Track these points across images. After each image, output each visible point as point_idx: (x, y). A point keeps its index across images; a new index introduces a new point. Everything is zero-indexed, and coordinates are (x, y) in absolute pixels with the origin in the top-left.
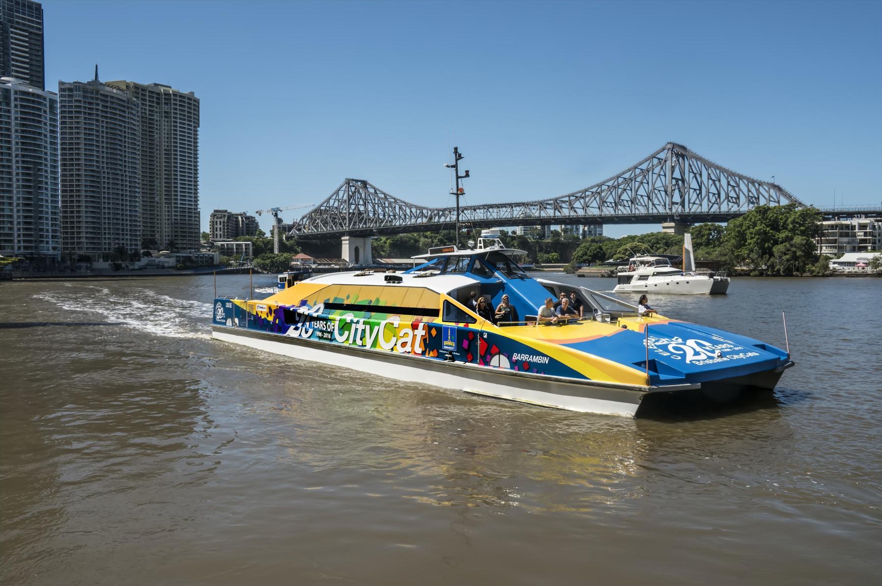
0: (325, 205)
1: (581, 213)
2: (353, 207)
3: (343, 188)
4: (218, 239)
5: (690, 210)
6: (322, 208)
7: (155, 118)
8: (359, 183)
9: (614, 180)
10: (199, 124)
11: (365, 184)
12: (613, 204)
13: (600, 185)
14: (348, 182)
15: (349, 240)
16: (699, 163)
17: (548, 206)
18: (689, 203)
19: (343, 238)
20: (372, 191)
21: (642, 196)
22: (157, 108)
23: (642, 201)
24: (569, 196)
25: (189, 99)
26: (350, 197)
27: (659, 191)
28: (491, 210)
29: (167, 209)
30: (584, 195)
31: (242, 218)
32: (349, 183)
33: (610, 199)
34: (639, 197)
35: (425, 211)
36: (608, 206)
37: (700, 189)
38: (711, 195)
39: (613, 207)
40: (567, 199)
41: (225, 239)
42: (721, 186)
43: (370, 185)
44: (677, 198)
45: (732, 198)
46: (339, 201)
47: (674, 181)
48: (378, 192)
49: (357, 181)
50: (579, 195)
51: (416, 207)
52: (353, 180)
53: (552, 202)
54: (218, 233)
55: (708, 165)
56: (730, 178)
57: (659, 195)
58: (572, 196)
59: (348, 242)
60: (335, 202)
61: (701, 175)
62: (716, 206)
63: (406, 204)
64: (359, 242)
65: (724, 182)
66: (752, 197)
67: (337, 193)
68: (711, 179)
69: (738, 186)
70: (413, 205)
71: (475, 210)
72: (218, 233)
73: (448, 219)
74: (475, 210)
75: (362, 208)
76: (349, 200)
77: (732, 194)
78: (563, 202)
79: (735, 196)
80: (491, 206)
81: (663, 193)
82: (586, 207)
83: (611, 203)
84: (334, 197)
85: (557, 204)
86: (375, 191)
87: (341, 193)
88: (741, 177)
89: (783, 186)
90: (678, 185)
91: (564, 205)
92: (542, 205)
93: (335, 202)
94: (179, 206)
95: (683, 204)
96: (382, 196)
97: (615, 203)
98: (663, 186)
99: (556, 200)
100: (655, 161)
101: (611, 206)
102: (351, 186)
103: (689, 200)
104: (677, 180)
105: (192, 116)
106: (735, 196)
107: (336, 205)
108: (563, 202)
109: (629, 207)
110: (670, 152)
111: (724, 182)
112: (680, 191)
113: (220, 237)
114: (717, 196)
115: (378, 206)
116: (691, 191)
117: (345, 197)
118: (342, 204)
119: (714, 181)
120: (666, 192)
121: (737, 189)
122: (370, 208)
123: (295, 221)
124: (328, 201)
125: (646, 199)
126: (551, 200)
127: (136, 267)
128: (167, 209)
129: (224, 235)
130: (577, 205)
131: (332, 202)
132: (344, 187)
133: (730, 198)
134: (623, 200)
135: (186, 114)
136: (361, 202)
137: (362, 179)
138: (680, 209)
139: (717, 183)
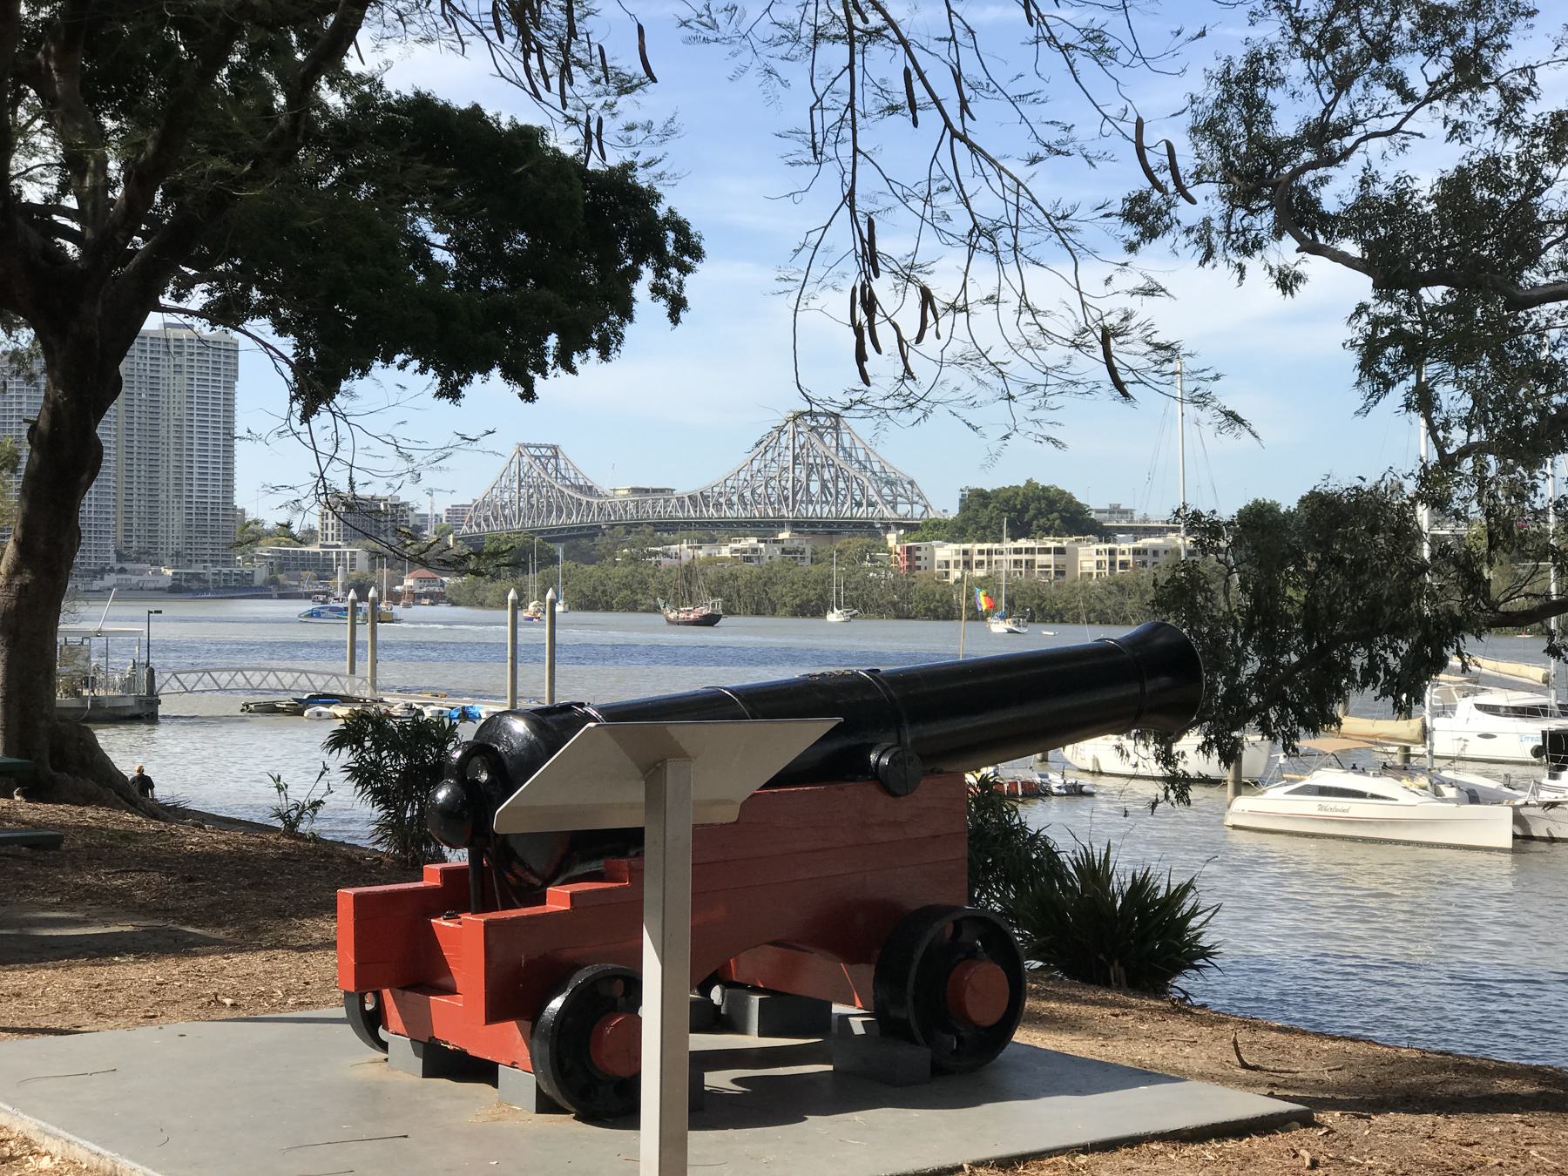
4: (330, 542)
7: (161, 375)
8: (543, 450)
10: (236, 377)
22: (164, 360)
25: (214, 342)
29: (176, 505)
31: (385, 505)
41: (340, 543)
49: (538, 447)
54: (330, 532)
72: (330, 532)
94: (194, 500)
105: (222, 366)
127: (95, 587)
128: (176, 505)
129: (339, 535)
135: (210, 365)
137: (549, 443)
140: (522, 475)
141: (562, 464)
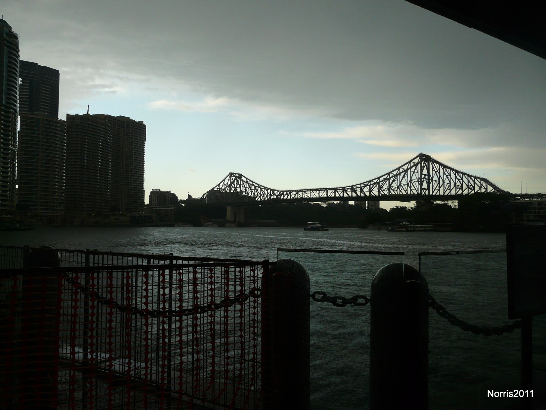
0: (217, 187)
1: (368, 194)
2: (233, 189)
4: (154, 206)
5: (433, 192)
6: (215, 189)
11: (240, 175)
12: (387, 189)
13: (379, 178)
14: (231, 174)
16: (438, 165)
17: (348, 190)
18: (433, 189)
19: (227, 207)
20: (244, 179)
21: (404, 184)
23: (404, 187)
24: (361, 184)
26: (231, 183)
27: (414, 181)
28: (315, 192)
30: (369, 183)
33: (385, 186)
34: (402, 185)
35: (275, 192)
36: (384, 190)
37: (439, 181)
38: (445, 184)
39: (387, 191)
40: (359, 186)
42: (451, 178)
43: (243, 176)
44: (425, 186)
45: (458, 186)
46: (225, 185)
47: (423, 176)
48: (248, 180)
49: (236, 174)
50: (366, 184)
51: (271, 190)
53: (351, 187)
55: (445, 167)
56: (457, 174)
57: (414, 184)
59: (230, 209)
60: (223, 186)
61: (439, 173)
62: (448, 191)
63: (265, 188)
65: (453, 176)
66: (470, 186)
67: (224, 180)
68: (446, 175)
69: (462, 179)
70: (269, 188)
71: (305, 192)
73: (289, 197)
74: (305, 192)
75: (238, 190)
77: (458, 184)
78: (357, 187)
79: (460, 185)
80: (315, 190)
81: (417, 183)
82: (370, 191)
83: (385, 188)
85: (353, 189)
86: (246, 180)
87: (226, 181)
88: (464, 174)
89: (489, 179)
90: (426, 178)
91: (357, 189)
92: (344, 189)
93: (223, 186)
95: (428, 189)
96: (251, 183)
97: (388, 188)
98: (417, 179)
99: (352, 186)
100: (412, 164)
101: (385, 190)
103: (432, 187)
104: (425, 175)
106: (460, 185)
107: (223, 187)
108: (357, 187)
109: (396, 191)
111: (453, 176)
112: (427, 182)
113: (155, 205)
114: (449, 185)
115: (248, 189)
116: (434, 182)
118: (227, 187)
119: (447, 176)
120: (418, 182)
121: (461, 181)
122: (243, 189)
123: (199, 196)
124: (219, 185)
125: (406, 186)
130: (366, 190)
131: (221, 186)
132: (229, 177)
133: (457, 186)
134: (392, 187)
136: (238, 186)
138: (427, 193)
139: (449, 177)
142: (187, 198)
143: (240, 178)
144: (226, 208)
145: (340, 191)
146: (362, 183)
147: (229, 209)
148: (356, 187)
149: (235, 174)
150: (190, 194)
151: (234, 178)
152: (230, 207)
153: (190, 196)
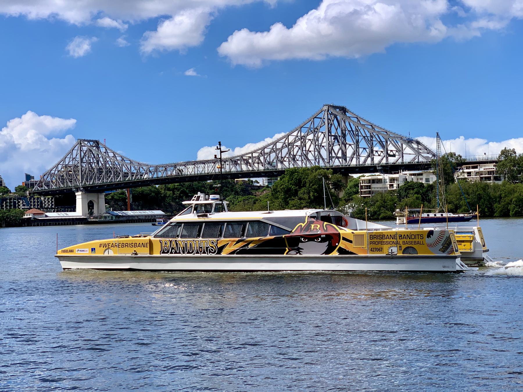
0: (62, 163)
3: (76, 148)
8: (92, 143)
9: (284, 139)
11: (97, 144)
15: (82, 195)
24: (252, 153)
32: (81, 144)
40: (250, 155)
48: (108, 151)
49: (89, 141)
52: (85, 140)
53: (239, 158)
58: (254, 152)
59: (80, 197)
64: (93, 197)
76: (82, 160)
84: (69, 156)
87: (75, 152)
99: (242, 156)
102: (82, 146)
108: (250, 157)
110: (326, 113)
117: (78, 156)
126: (238, 156)
132: (77, 146)
133: (374, 152)
137: (94, 139)
140: (82, 154)
141: (103, 150)
142: (24, 180)
143: (98, 147)
144: (75, 196)
145: (228, 165)
146: (255, 152)
147: (79, 197)
148: (249, 157)
149: (86, 143)
150: (28, 174)
151: (85, 149)
152: (80, 193)
153: (28, 177)
